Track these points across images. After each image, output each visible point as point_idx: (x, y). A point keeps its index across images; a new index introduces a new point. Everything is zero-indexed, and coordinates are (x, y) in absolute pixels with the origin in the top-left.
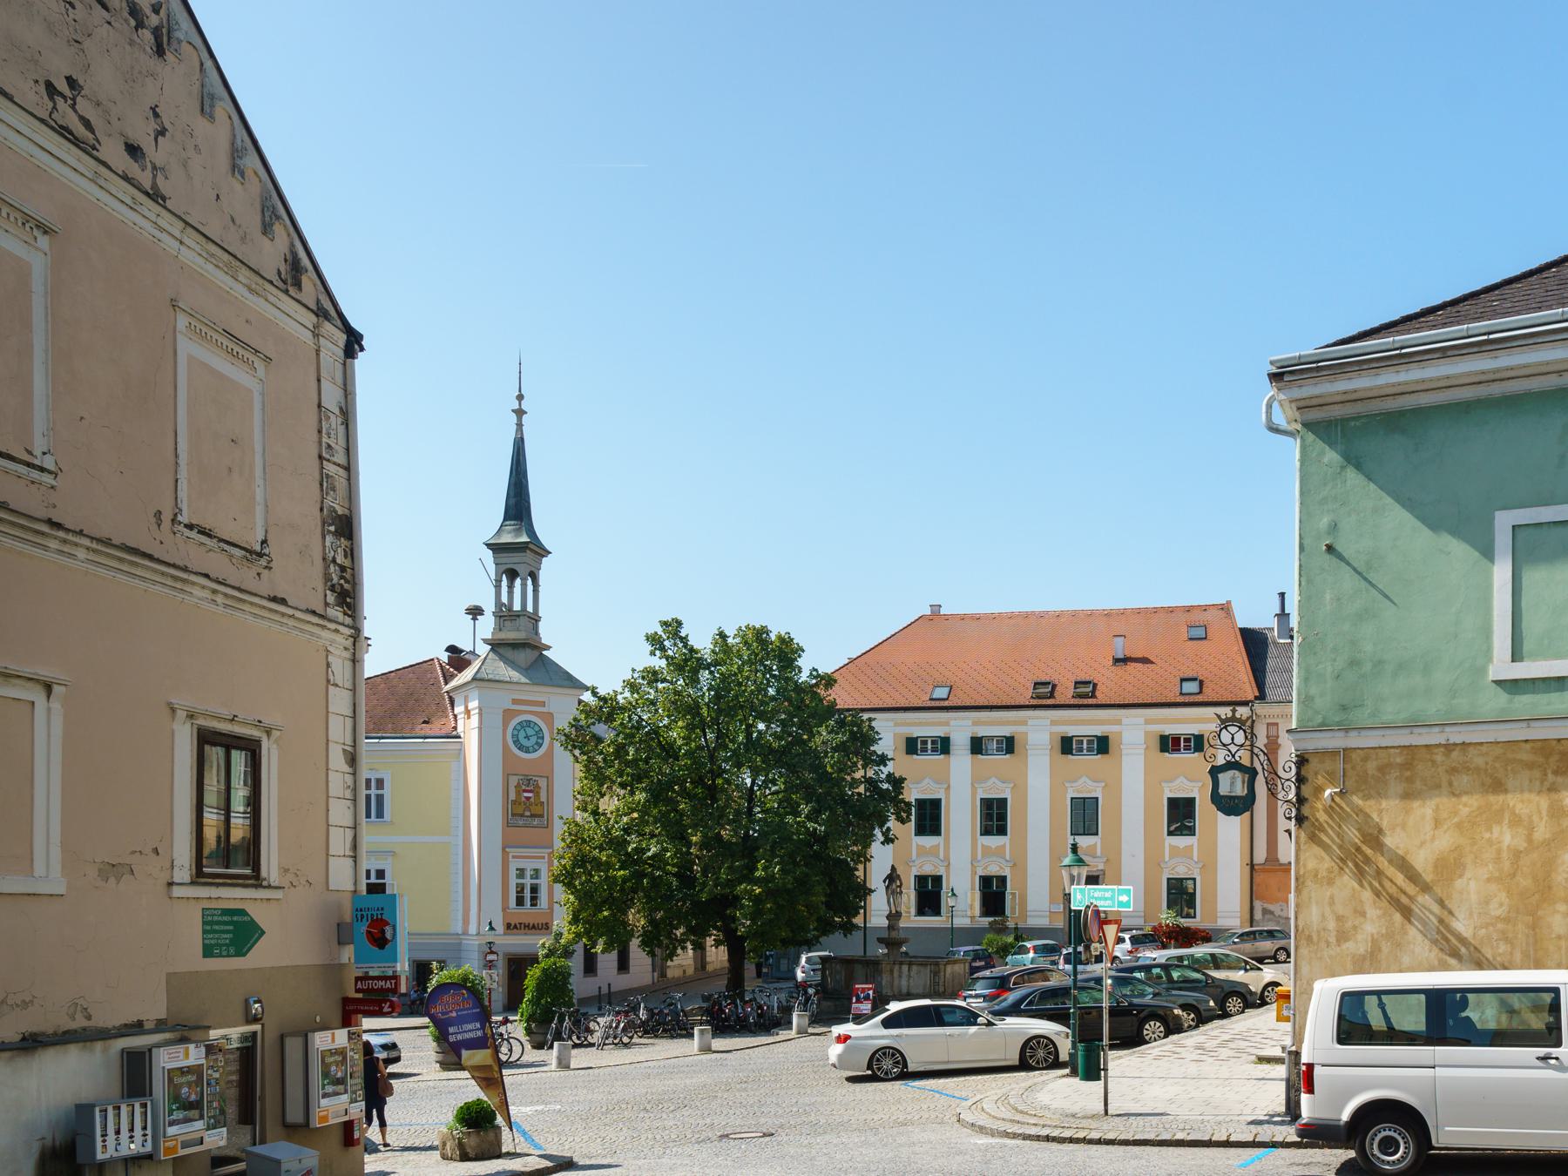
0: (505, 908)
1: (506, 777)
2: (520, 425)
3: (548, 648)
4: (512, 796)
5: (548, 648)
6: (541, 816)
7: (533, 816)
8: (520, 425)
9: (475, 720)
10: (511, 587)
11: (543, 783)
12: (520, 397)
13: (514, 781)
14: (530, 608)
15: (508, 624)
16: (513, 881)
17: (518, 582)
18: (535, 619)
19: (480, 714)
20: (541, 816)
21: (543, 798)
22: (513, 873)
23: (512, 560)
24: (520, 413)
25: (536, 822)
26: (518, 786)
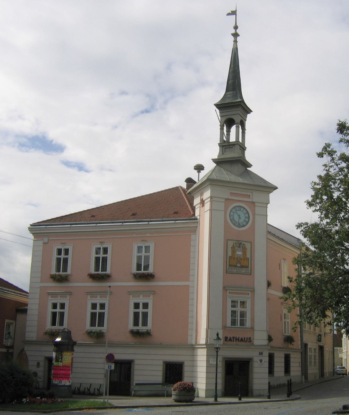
0: (224, 327)
1: (226, 241)
2: (235, 41)
3: (250, 166)
4: (230, 254)
5: (250, 166)
6: (247, 267)
7: (242, 267)
8: (235, 41)
9: (207, 206)
10: (229, 131)
11: (248, 246)
12: (236, 28)
13: (231, 244)
14: (240, 141)
15: (227, 150)
16: (229, 309)
17: (233, 129)
18: (243, 149)
19: (211, 201)
20: (247, 267)
21: (248, 256)
22: (229, 304)
23: (230, 114)
24: (236, 35)
25: (244, 271)
26: (233, 247)
